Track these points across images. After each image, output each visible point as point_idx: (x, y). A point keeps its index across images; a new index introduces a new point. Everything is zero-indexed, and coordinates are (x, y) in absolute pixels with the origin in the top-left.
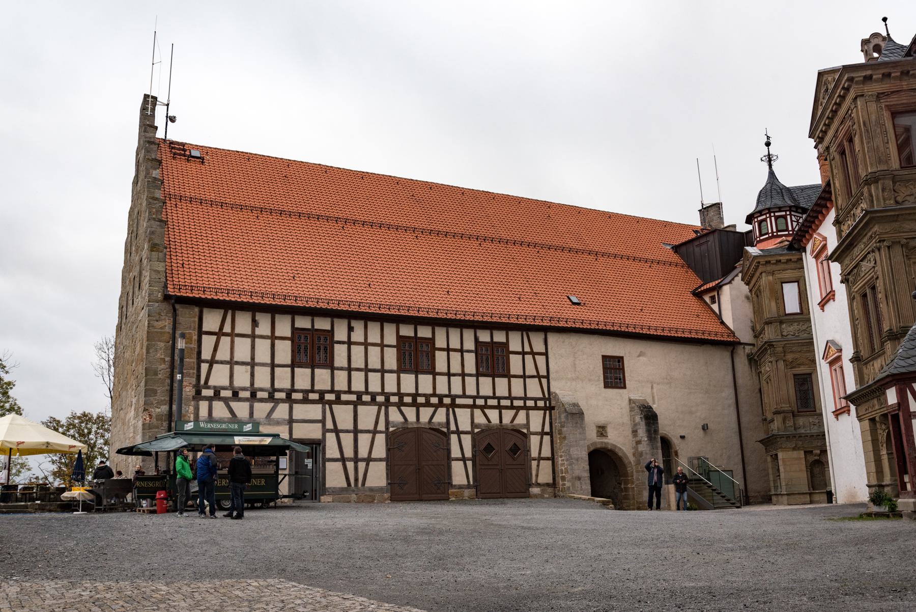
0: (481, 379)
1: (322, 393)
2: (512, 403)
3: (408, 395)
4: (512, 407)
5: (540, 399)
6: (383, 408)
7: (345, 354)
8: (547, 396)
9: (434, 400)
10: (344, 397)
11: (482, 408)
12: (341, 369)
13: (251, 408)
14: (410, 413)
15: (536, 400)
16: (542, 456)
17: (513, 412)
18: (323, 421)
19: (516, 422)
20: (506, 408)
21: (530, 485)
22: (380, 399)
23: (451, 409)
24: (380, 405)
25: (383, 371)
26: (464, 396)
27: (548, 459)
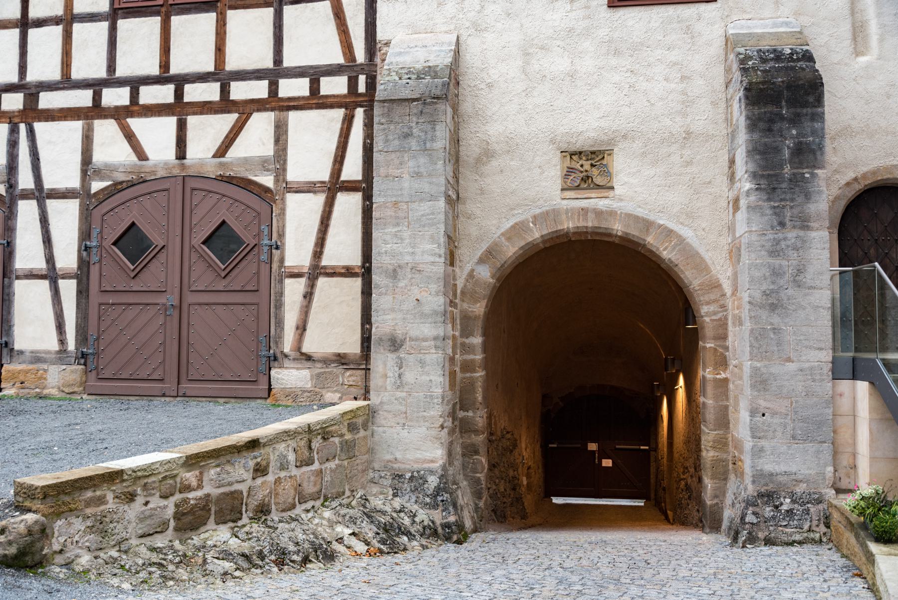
0: (123, 24)
2: (225, 91)
4: (225, 105)
5: (333, 71)
8: (360, 56)
11: (120, 114)
15: (315, 74)
16: (325, 262)
17: (226, 121)
19: (236, 152)
20: (205, 108)
21: (274, 359)
23: (22, 127)
26: (67, 83)
27: (348, 272)
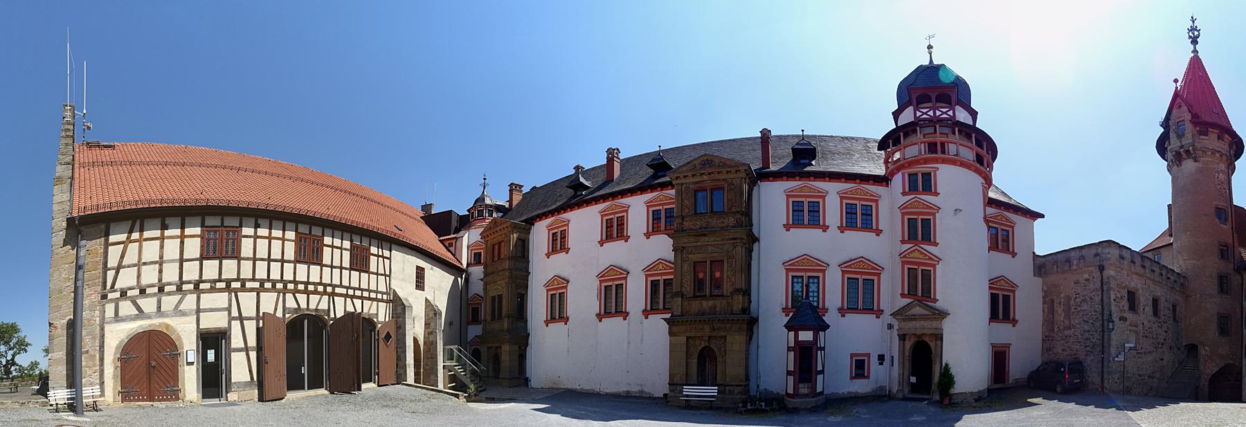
1: (228, 282)
3: (302, 283)
6: (282, 294)
7: (252, 246)
9: (321, 288)
10: (249, 285)
12: (248, 259)
13: (159, 302)
14: (302, 298)
18: (229, 309)
22: (280, 286)
24: (279, 292)
25: (283, 261)
